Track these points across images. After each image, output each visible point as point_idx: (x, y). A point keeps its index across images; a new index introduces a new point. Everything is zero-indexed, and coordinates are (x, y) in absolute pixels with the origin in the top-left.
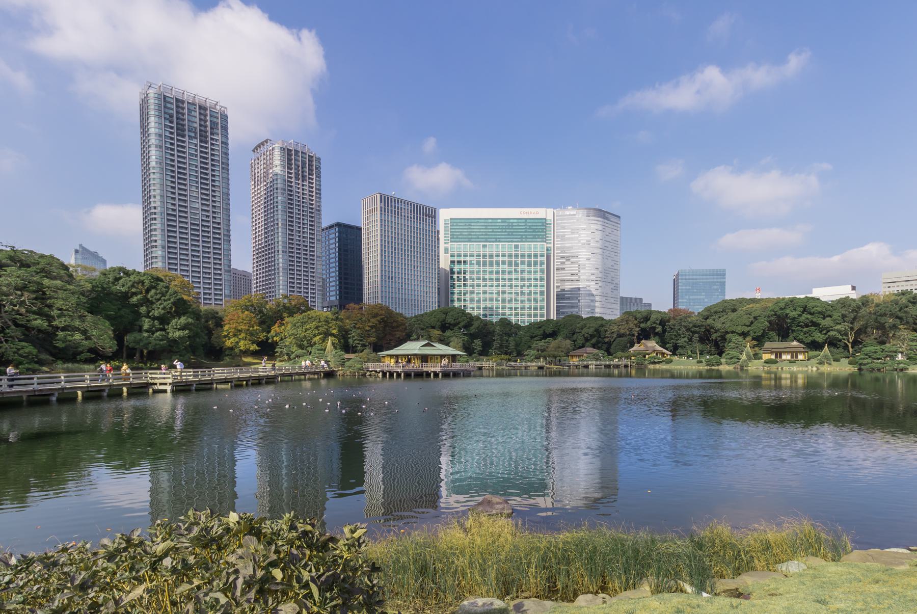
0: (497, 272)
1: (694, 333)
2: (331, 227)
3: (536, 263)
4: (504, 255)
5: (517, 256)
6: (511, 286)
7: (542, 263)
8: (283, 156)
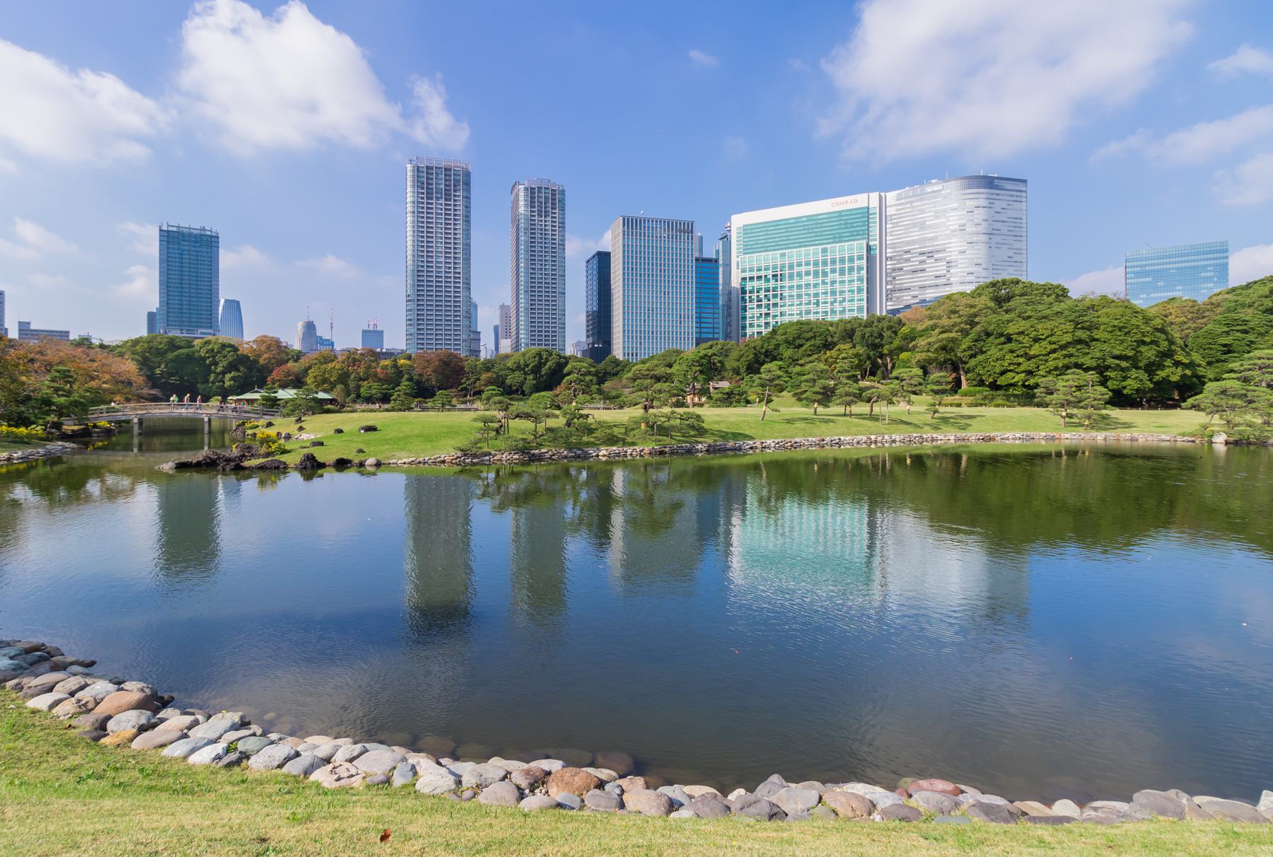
0: (799, 287)
3: (851, 269)
4: (808, 264)
5: (825, 263)
6: (817, 304)
7: (860, 269)
8: (526, 196)
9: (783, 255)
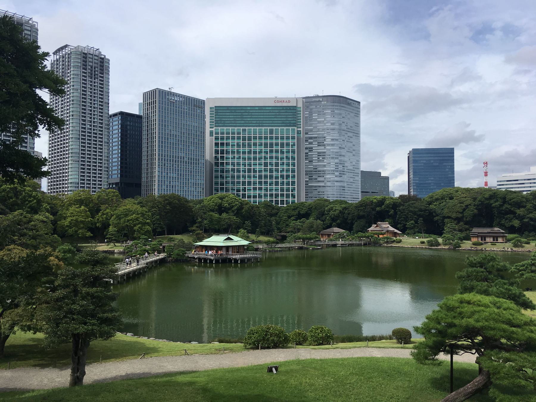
1: (420, 216)
2: (115, 115)
9: (244, 130)
